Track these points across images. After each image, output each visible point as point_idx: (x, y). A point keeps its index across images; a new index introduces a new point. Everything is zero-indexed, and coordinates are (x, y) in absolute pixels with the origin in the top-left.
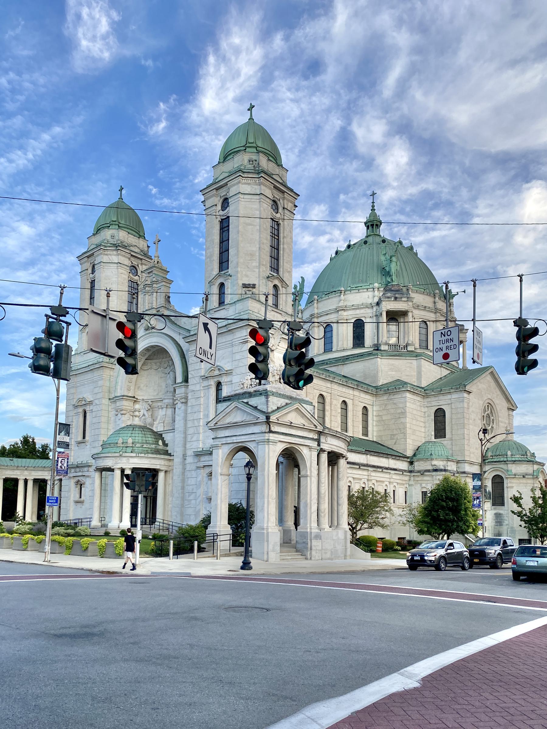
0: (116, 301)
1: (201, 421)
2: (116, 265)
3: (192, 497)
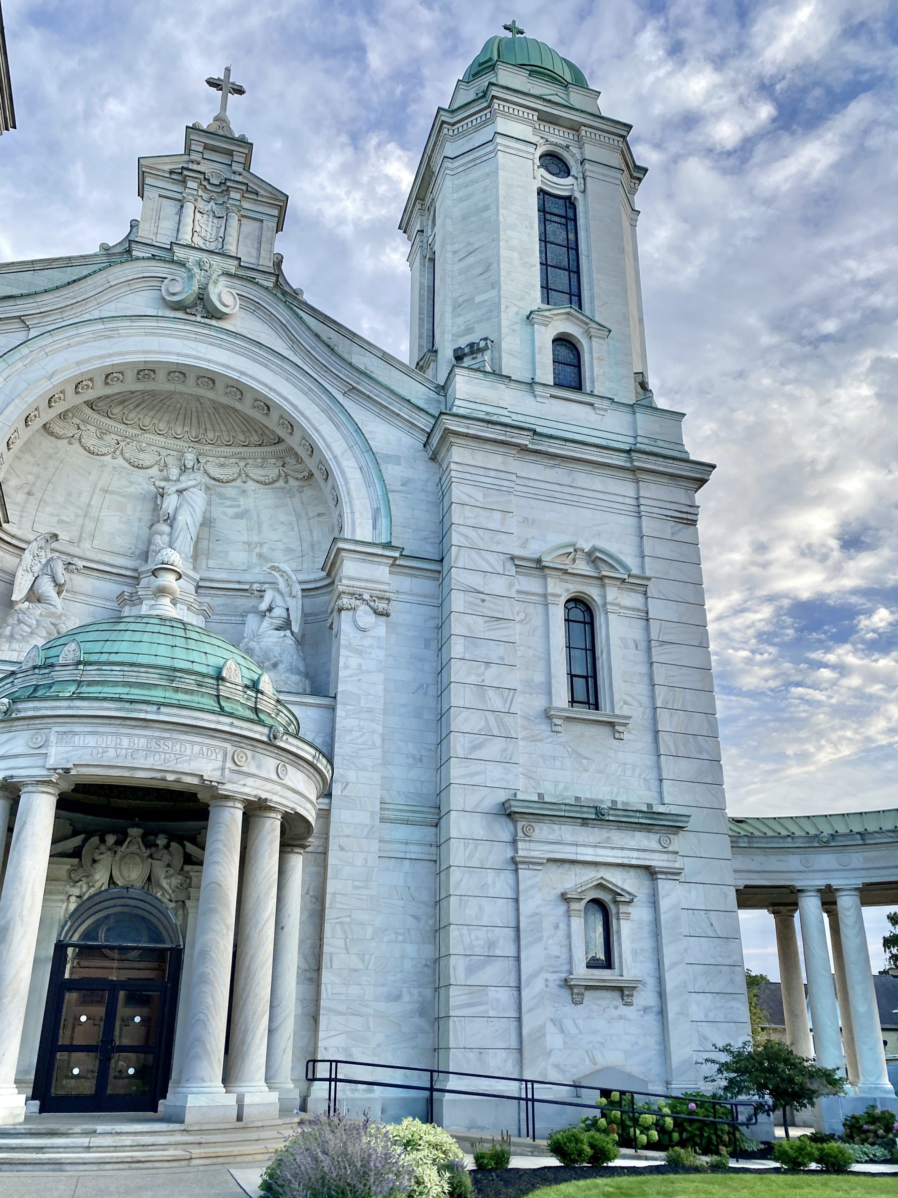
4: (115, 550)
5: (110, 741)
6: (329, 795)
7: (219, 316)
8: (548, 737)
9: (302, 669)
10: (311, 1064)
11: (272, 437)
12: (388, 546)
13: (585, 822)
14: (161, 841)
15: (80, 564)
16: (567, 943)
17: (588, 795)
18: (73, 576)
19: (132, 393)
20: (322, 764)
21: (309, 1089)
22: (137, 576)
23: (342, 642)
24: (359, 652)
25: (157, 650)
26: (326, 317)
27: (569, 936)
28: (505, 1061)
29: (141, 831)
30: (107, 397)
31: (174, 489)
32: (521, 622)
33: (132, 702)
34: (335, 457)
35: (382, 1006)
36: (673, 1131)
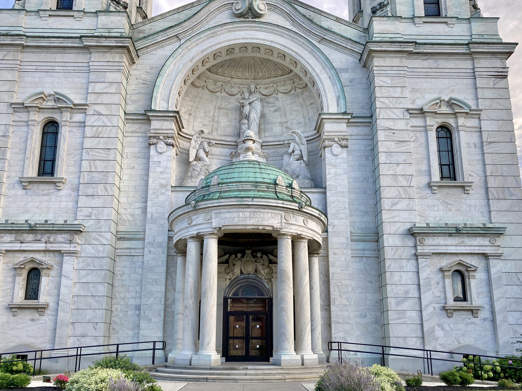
4: (227, 134)
5: (235, 215)
6: (327, 231)
7: (259, 16)
8: (430, 196)
9: (309, 177)
10: (330, 344)
11: (287, 70)
12: (345, 113)
13: (450, 235)
14: (259, 255)
15: (214, 142)
16: (443, 290)
17: (452, 222)
18: (211, 148)
19: (225, 61)
20: (323, 218)
21: (329, 354)
22: (237, 144)
23: (327, 162)
24: (335, 166)
25: (249, 175)
26: (308, 5)
27: (444, 287)
28: (416, 342)
29: (251, 251)
30: (215, 65)
31: (248, 103)
32: (413, 141)
33: (242, 198)
34: (317, 74)
35: (358, 320)
36: (501, 373)
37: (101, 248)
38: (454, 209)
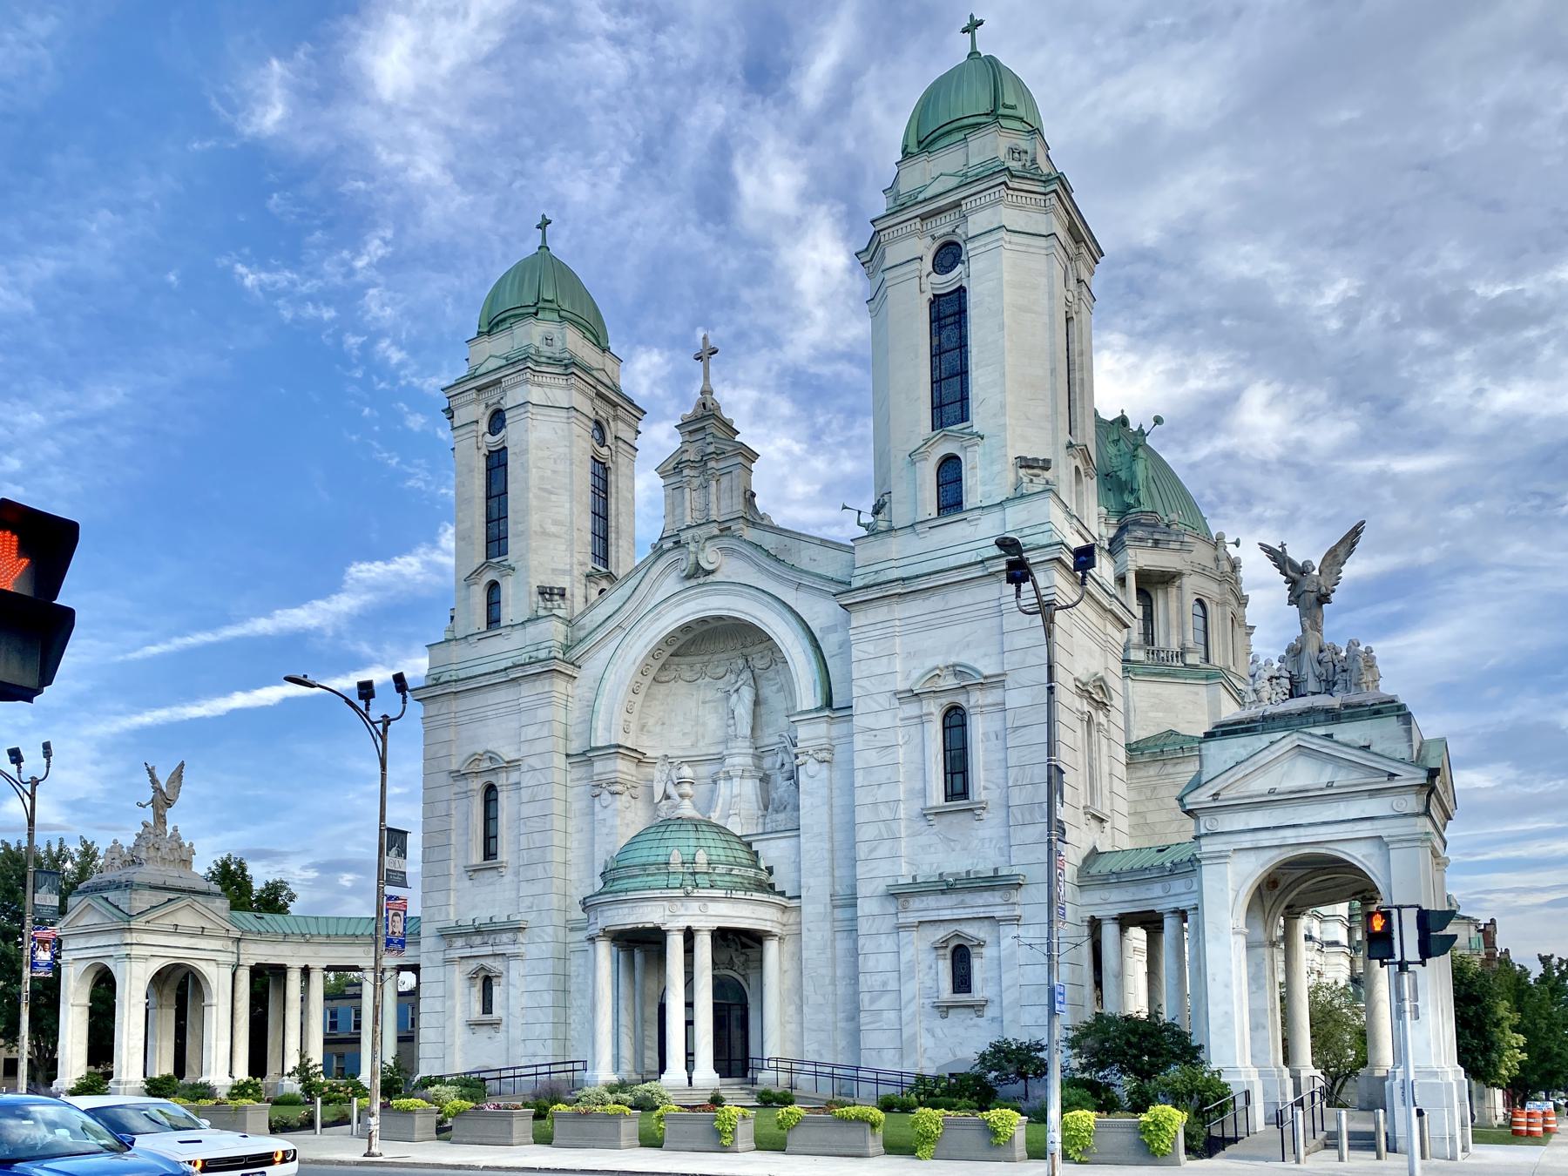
0: (568, 505)
1: (902, 806)
2: (563, 413)
3: (883, 1003)
13: (943, 892)
37: (544, 947)
38: (958, 848)
